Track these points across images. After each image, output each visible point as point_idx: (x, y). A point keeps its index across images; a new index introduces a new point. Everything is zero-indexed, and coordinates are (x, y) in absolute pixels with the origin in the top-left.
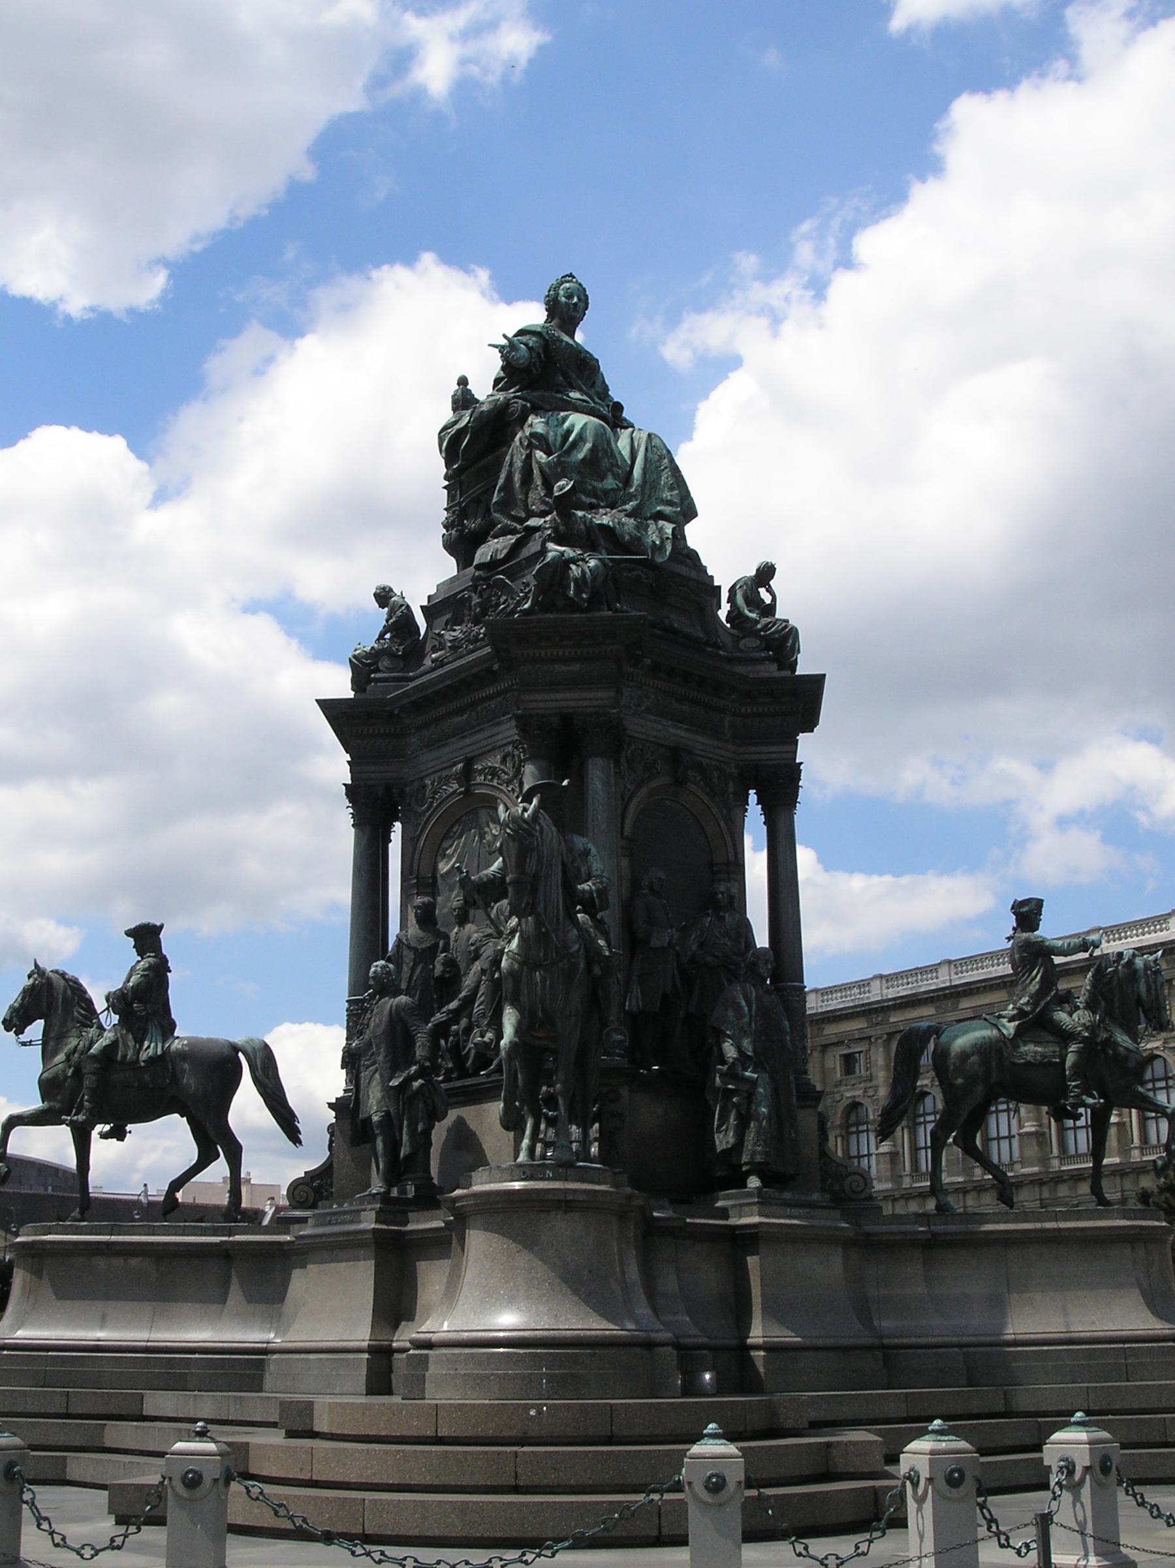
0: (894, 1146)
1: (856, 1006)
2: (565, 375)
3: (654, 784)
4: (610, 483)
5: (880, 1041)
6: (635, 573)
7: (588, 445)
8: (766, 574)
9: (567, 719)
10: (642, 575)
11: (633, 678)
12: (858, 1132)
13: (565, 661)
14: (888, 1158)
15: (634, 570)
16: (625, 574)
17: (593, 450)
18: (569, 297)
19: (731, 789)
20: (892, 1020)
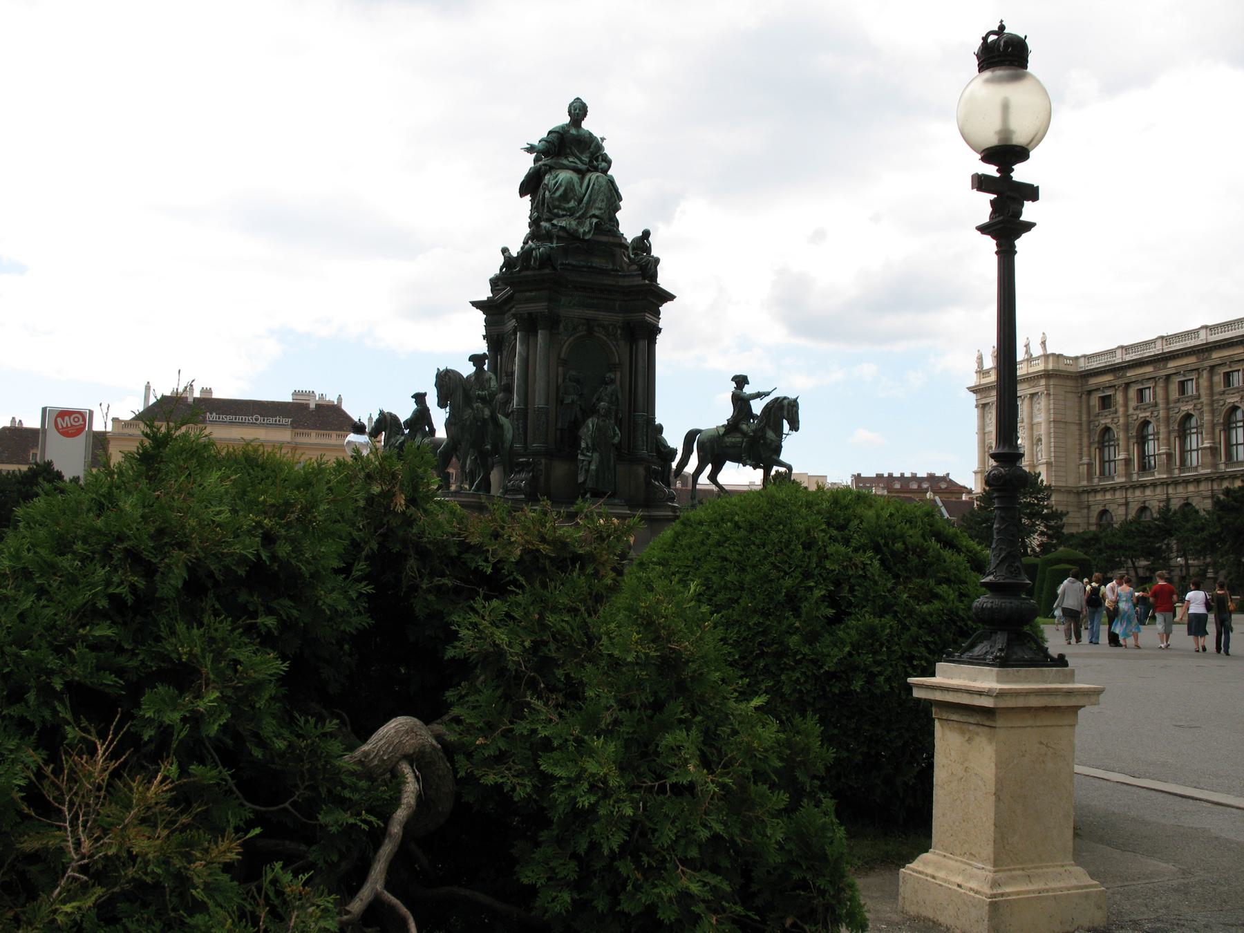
0: (1129, 455)
1: (1105, 366)
2: (570, 149)
3: (578, 335)
4: (572, 204)
5: (1121, 388)
7: (563, 188)
8: (646, 234)
9: (530, 314)
12: (1109, 446)
13: (530, 291)
14: (1123, 462)
17: (565, 190)
18: (575, 110)
19: (619, 332)
20: (1128, 375)
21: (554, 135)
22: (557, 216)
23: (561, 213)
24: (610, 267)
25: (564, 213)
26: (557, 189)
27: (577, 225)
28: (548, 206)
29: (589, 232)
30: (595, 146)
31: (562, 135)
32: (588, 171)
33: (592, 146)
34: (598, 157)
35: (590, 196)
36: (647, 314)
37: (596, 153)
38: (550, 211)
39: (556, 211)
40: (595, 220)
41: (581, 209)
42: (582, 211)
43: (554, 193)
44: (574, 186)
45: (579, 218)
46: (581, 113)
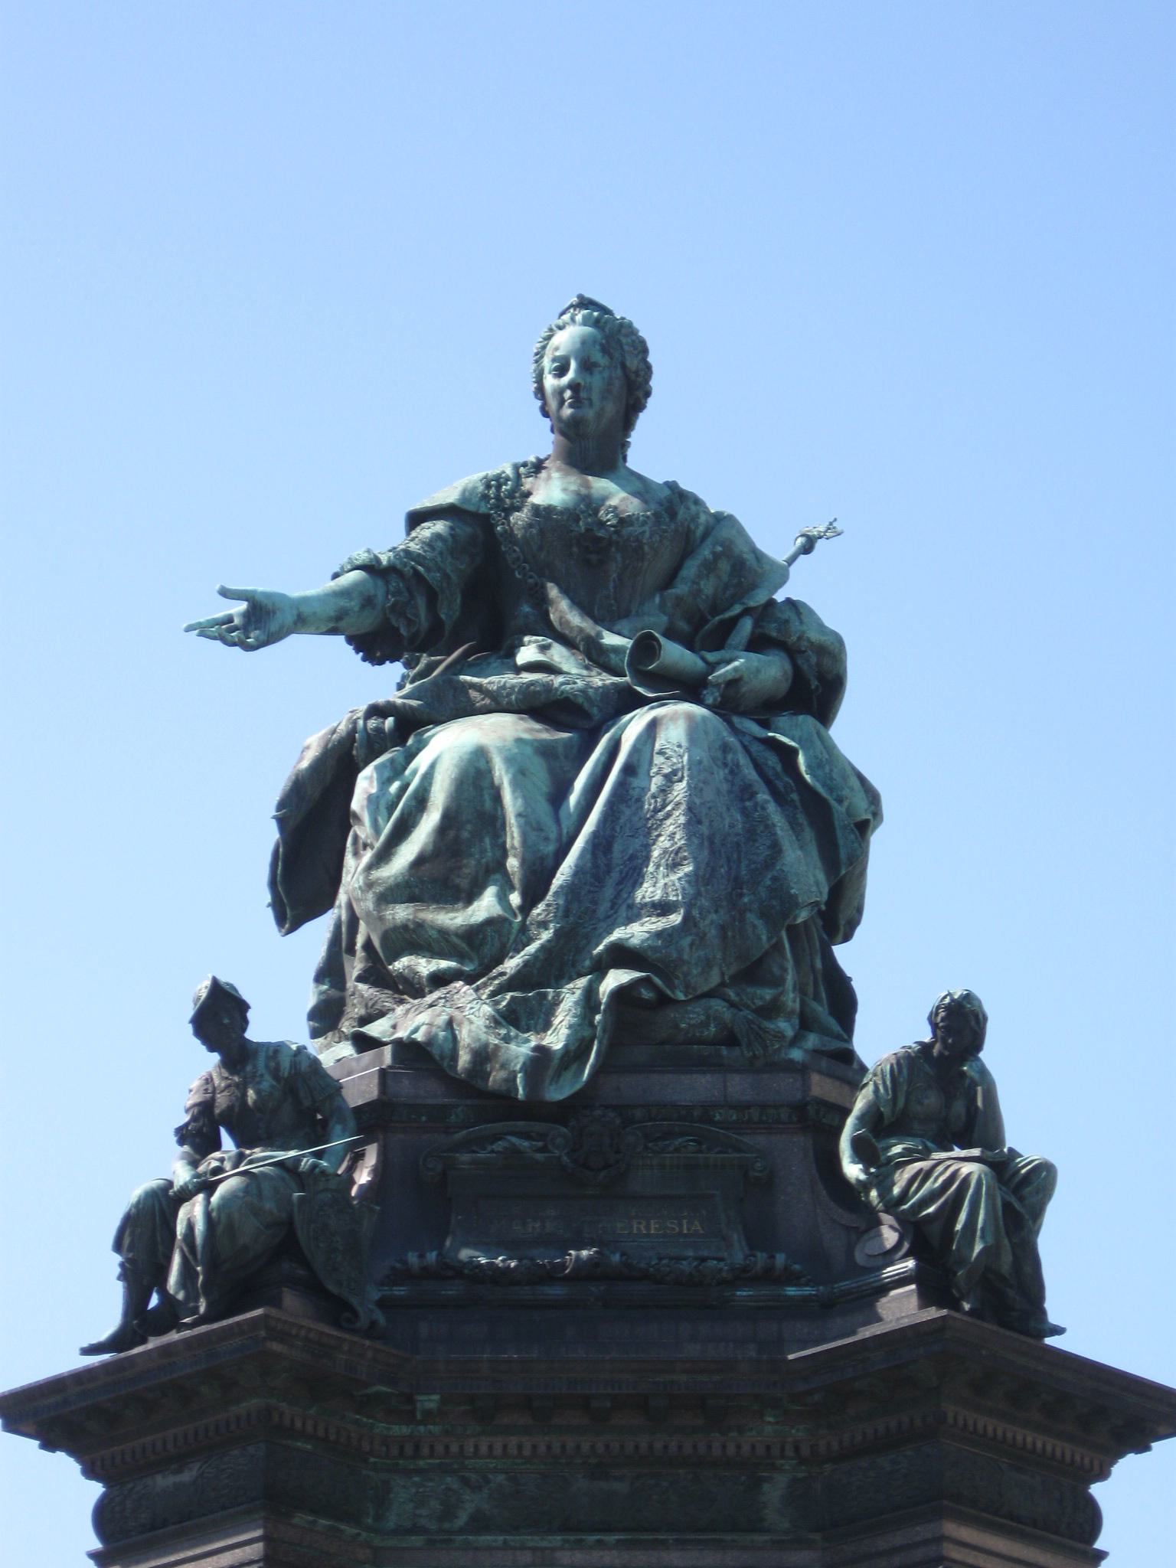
4: (486, 906)
6: (499, 1146)
10: (526, 1144)
11: (417, 1448)
13: (178, 1460)
15: (496, 1138)
16: (466, 1157)
18: (561, 370)
21: (439, 526)
22: (410, 988)
23: (424, 966)
24: (739, 1257)
25: (444, 964)
26: (402, 831)
27: (496, 1022)
28: (368, 945)
29: (575, 1053)
30: (709, 567)
31: (484, 522)
32: (630, 701)
33: (690, 569)
34: (733, 622)
35: (600, 844)
36: (951, 1528)
37: (715, 610)
38: (377, 975)
39: (400, 964)
40: (616, 978)
41: (544, 925)
42: (546, 935)
43: (384, 855)
44: (497, 798)
45: (519, 981)
46: (597, 381)
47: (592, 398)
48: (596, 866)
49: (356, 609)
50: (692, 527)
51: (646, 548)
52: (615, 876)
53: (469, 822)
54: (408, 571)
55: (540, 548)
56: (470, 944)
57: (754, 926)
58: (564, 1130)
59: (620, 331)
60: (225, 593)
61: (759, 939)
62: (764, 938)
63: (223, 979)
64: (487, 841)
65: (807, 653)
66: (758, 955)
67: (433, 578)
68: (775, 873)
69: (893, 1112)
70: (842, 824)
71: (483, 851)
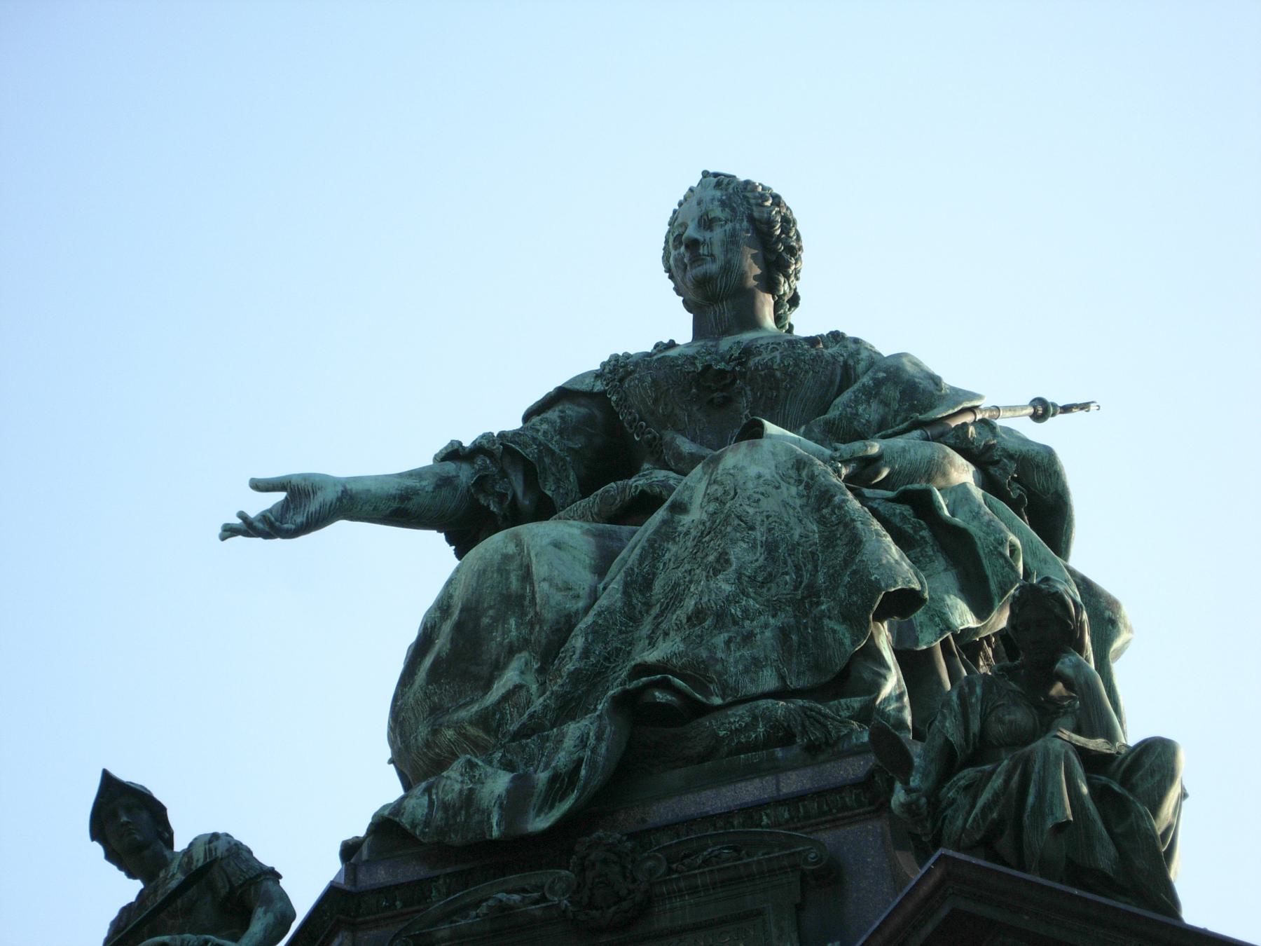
47: (714, 253)
48: (628, 604)
49: (430, 489)
50: (851, 362)
51: (778, 374)
52: (656, 610)
53: (490, 607)
54: (498, 448)
55: (656, 401)
56: (487, 730)
57: (834, 631)
58: (564, 873)
59: (745, 189)
60: (260, 486)
61: (842, 644)
62: (847, 642)
63: (124, 774)
64: (512, 622)
65: (1001, 462)
66: (840, 664)
67: (531, 452)
68: (854, 567)
69: (967, 740)
70: (987, 550)
71: (506, 632)
